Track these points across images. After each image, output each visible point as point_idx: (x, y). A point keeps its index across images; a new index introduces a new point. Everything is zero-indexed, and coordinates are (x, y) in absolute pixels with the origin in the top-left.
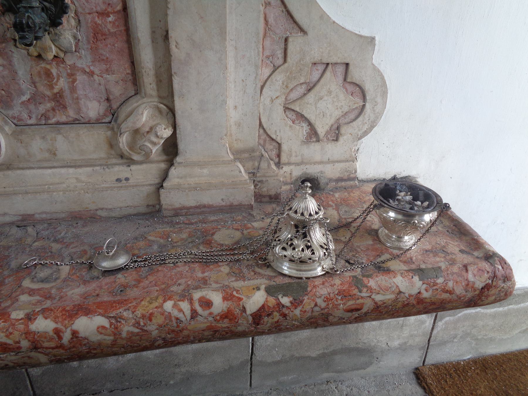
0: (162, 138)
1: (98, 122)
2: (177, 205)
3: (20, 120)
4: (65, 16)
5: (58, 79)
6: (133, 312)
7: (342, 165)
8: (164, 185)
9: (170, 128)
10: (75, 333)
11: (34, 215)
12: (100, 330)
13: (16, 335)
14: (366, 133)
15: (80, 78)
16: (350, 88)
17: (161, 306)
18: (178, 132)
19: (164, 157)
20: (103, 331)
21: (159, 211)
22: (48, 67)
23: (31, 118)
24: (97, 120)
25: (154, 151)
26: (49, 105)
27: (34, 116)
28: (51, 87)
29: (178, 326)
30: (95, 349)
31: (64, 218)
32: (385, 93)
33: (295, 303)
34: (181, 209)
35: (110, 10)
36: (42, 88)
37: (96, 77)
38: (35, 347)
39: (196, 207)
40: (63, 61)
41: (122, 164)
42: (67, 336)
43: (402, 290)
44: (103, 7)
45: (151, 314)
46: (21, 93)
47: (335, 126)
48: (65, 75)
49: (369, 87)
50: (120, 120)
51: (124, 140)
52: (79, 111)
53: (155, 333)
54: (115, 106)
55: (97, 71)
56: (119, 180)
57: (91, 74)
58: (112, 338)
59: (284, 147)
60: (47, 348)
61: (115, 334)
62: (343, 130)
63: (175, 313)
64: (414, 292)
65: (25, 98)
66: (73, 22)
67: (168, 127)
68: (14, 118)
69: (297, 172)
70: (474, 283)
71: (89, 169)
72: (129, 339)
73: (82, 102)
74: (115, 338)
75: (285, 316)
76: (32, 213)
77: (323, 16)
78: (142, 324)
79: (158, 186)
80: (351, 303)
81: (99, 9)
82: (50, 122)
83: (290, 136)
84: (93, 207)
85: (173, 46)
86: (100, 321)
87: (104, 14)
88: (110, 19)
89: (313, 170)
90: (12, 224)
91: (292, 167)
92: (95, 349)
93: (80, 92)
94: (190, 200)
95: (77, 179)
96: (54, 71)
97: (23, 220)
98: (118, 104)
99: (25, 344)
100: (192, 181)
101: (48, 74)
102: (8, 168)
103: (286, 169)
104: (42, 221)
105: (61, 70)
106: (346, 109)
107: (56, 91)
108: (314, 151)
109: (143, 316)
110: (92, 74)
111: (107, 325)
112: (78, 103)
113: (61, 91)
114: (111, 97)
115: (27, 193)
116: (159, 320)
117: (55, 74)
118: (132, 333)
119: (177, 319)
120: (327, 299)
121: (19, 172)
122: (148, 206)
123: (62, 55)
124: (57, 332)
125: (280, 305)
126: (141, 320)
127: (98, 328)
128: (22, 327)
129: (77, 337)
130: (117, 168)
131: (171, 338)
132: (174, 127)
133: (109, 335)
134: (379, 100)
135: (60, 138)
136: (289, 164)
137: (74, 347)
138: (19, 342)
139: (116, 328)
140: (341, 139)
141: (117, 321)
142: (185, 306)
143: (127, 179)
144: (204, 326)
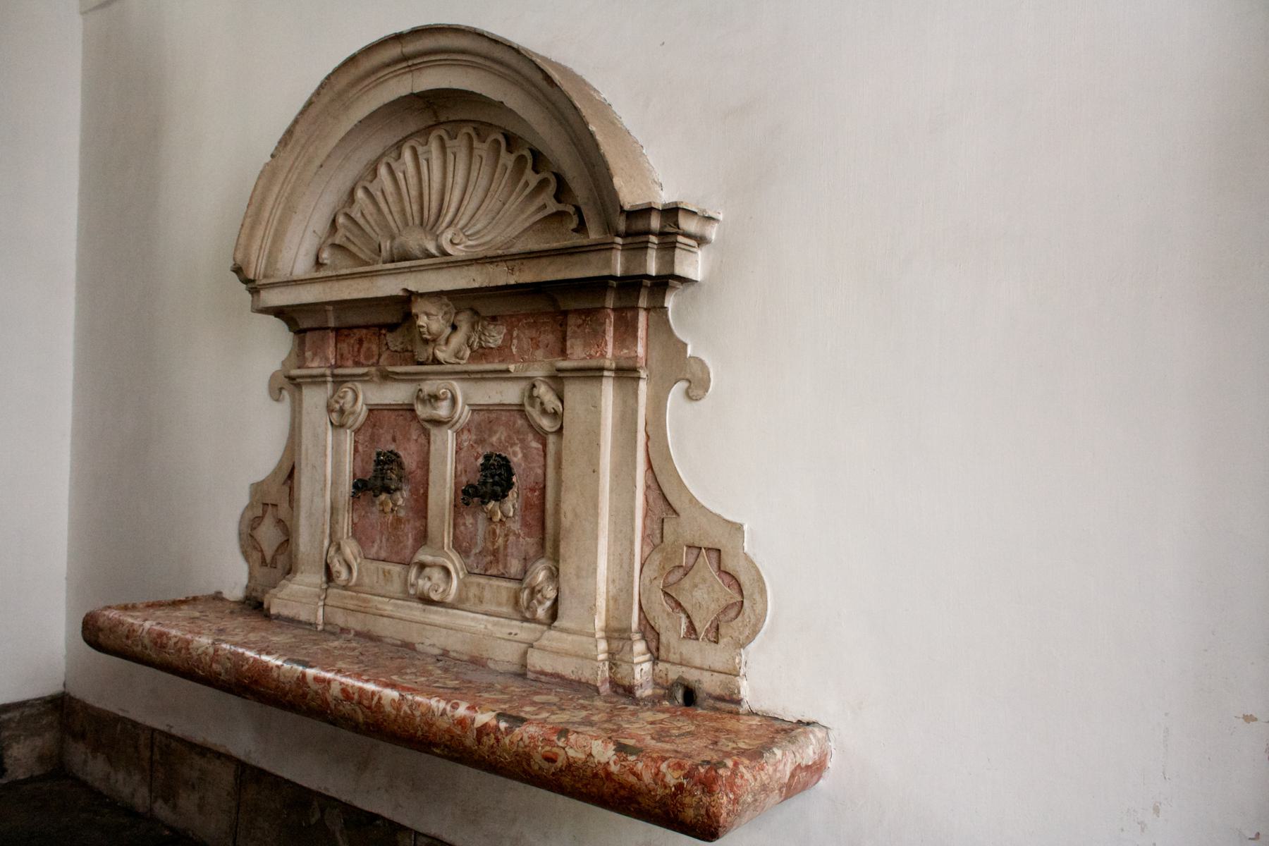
7: (723, 677)
14: (750, 639)
15: (512, 538)
16: (727, 579)
26: (490, 558)
28: (493, 543)
32: (763, 591)
33: (509, 731)
34: (542, 673)
36: (489, 544)
38: (360, 703)
39: (552, 675)
43: (594, 753)
47: (714, 625)
49: (744, 579)
52: (505, 567)
57: (518, 536)
59: (663, 639)
62: (722, 631)
64: (603, 760)
69: (674, 673)
70: (664, 775)
75: (498, 740)
77: (693, 501)
80: (548, 748)
83: (671, 629)
84: (485, 655)
86: (395, 694)
87: (533, 490)
89: (692, 676)
91: (668, 665)
96: (498, 531)
99: (356, 697)
100: (554, 644)
101: (494, 532)
103: (661, 666)
106: (724, 603)
108: (691, 650)
116: (423, 709)
120: (531, 737)
125: (497, 728)
134: (757, 597)
136: (668, 662)
140: (723, 641)
142: (442, 705)
144: (446, 726)
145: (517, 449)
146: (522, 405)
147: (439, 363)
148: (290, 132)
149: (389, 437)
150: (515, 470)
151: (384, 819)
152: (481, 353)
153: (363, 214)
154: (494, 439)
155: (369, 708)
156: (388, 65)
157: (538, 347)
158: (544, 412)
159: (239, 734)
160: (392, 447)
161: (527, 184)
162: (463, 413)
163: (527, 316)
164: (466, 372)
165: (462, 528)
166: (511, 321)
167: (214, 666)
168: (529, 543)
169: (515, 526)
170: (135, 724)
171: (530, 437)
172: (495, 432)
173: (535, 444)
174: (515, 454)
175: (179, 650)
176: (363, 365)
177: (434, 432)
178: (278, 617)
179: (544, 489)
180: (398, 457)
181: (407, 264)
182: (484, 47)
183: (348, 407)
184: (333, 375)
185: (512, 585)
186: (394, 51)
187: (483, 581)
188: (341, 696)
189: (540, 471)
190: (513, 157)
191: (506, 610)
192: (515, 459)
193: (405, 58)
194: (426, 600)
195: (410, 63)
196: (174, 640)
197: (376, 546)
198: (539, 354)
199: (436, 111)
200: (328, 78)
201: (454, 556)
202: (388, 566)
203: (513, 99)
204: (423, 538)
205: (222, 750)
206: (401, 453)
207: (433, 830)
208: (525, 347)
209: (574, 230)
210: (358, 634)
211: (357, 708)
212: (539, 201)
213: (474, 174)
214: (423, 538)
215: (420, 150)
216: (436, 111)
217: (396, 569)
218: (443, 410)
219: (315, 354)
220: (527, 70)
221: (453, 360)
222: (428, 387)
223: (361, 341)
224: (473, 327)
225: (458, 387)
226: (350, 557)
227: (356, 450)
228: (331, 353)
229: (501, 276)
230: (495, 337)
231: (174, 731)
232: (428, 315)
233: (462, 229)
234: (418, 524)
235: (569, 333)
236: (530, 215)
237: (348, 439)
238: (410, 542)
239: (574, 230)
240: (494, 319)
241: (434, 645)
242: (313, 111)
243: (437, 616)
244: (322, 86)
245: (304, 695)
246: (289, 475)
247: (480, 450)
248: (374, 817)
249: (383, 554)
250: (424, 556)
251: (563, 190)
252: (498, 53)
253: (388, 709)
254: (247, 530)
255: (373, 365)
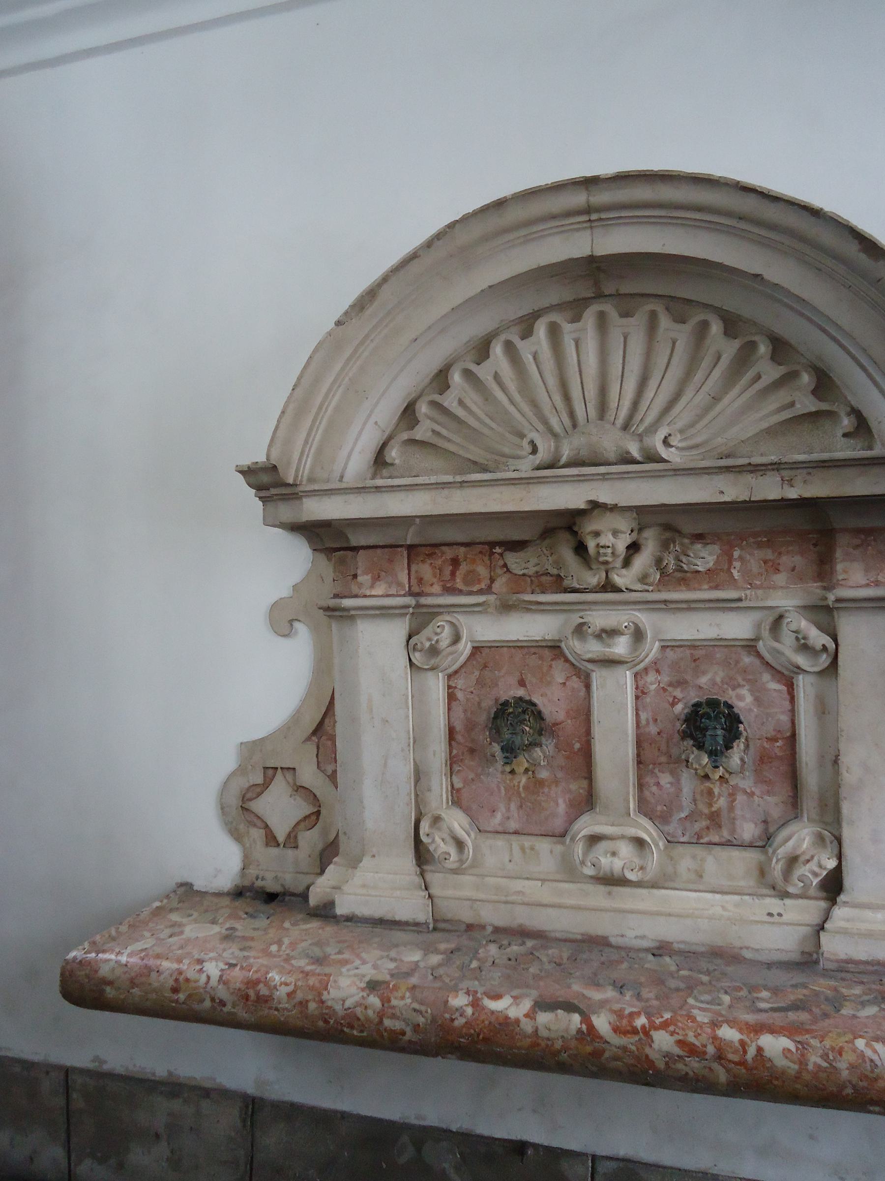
0: (825, 869)
1: (751, 846)
2: (842, 956)
3: (673, 837)
4: (737, 741)
5: (719, 798)
6: (821, 1042)
8: (826, 926)
9: (835, 859)
10: (760, 1050)
11: (672, 943)
12: (786, 1052)
13: (704, 1038)
15: (740, 798)
17: (852, 1042)
18: (843, 863)
19: (824, 894)
20: (789, 1055)
21: (817, 962)
22: (712, 786)
23: (684, 835)
24: (751, 842)
25: (814, 884)
26: (704, 823)
27: (688, 834)
28: (710, 805)
29: (872, 1071)
30: (777, 1079)
31: (702, 953)
35: (779, 736)
37: (756, 798)
38: (720, 1057)
39: (867, 963)
40: (727, 782)
41: (774, 896)
42: (752, 1052)
44: (773, 733)
45: (842, 1048)
46: (681, 808)
48: (726, 794)
50: (775, 844)
51: (777, 868)
52: (733, 831)
53: (845, 1074)
54: (771, 830)
55: (757, 792)
56: (770, 915)
57: (752, 794)
58: (796, 1067)
60: (730, 1061)
61: (801, 1063)
63: (869, 1053)
65: (683, 815)
66: (742, 746)
67: (832, 858)
68: (668, 834)
71: (737, 898)
72: (815, 1075)
73: (738, 823)
74: (800, 1068)
76: (671, 940)
78: (831, 1058)
79: (817, 928)
81: (769, 735)
82: (702, 841)
84: (738, 944)
85: (843, 770)
86: (785, 1042)
87: (773, 740)
88: (778, 744)
90: (647, 950)
92: (777, 1079)
93: (738, 812)
94: (861, 951)
95: (723, 907)
96: (716, 791)
97: (658, 948)
98: (776, 827)
99: (711, 1050)
100: (864, 926)
101: (710, 792)
102: (653, 887)
104: (680, 952)
105: (723, 789)
107: (713, 809)
109: (833, 1049)
110: (752, 794)
111: (794, 1050)
112: (734, 824)
113: (719, 809)
114: (769, 820)
115: (670, 915)
116: (849, 1057)
117: (716, 793)
118: (819, 1066)
119: (872, 1061)
121: (663, 891)
122: (803, 953)
123: (727, 776)
124: (742, 1043)
126: (830, 1052)
127: (784, 1049)
128: (709, 1030)
129: (762, 1056)
130: (768, 900)
131: (863, 1088)
132: (840, 857)
133: (795, 1063)
135: (710, 860)
137: (756, 1068)
138: (705, 1046)
139: (803, 1055)
141: (804, 1048)
143: (780, 915)
145: (744, 691)
146: (756, 640)
147: (617, 590)
148: (371, 294)
149: (513, 680)
150: (742, 718)
151: (535, 1146)
152: (683, 577)
153: (461, 402)
154: (703, 680)
155: (742, 1063)
156: (554, 217)
157: (778, 571)
158: (804, 647)
159: (244, 1065)
160: (521, 692)
161: (758, 377)
162: (651, 650)
163: (755, 535)
164: (665, 602)
165: (654, 789)
166: (728, 543)
167: (387, 1022)
168: (774, 804)
169: (746, 782)
170: (28, 1065)
171: (766, 677)
172: (704, 673)
173: (774, 686)
174: (741, 698)
175: (303, 1004)
176: (460, 592)
177: (598, 676)
178: (350, 918)
179: (793, 739)
180: (534, 705)
181: (602, 469)
182: (749, 205)
183: (444, 644)
184: (418, 606)
185: (752, 856)
186: (579, 199)
187: (699, 851)
188: (677, 1051)
189: (785, 718)
190: (736, 344)
191: (748, 883)
192: (741, 704)
193: (588, 210)
194: (613, 881)
195: (594, 217)
196: (283, 991)
197: (499, 816)
198: (780, 579)
199: (598, 282)
200: (452, 226)
201: (644, 821)
202: (527, 842)
203: (780, 271)
204: (588, 801)
205: (208, 1085)
206: (535, 700)
207: (622, 1152)
208: (755, 570)
209: (845, 435)
210: (497, 930)
211: (715, 1066)
212: (782, 396)
213: (661, 361)
214: (588, 801)
215: (567, 327)
216: (598, 282)
217: (544, 846)
218: (621, 647)
219: (377, 578)
220: (828, 237)
221: (639, 587)
222: (599, 619)
223: (455, 562)
224: (665, 545)
225: (644, 619)
226: (461, 834)
227: (451, 697)
228: (403, 577)
229: (731, 490)
230: (705, 557)
231: (106, 1067)
232: (615, 533)
233: (626, 427)
234: (573, 786)
235: (839, 554)
236: (769, 413)
237: (437, 686)
238: (562, 808)
239: (845, 435)
240: (699, 537)
241: (643, 937)
242: (415, 268)
243: (626, 898)
244: (439, 236)
245: (597, 1054)
246: (322, 729)
247: (678, 693)
248: (520, 1148)
249: (513, 825)
250: (586, 825)
251: (825, 384)
252: (771, 213)
253: (781, 1062)
254: (234, 801)
255: (481, 592)
